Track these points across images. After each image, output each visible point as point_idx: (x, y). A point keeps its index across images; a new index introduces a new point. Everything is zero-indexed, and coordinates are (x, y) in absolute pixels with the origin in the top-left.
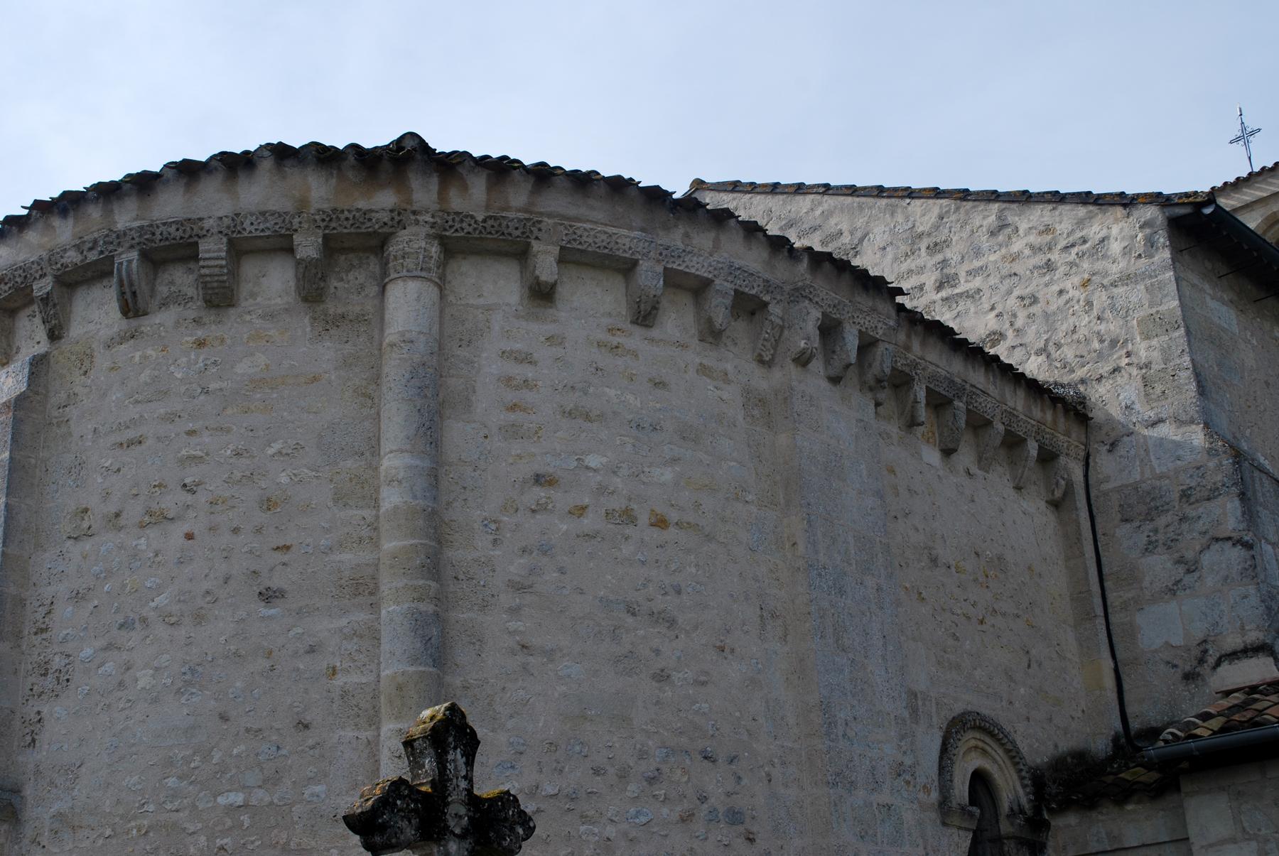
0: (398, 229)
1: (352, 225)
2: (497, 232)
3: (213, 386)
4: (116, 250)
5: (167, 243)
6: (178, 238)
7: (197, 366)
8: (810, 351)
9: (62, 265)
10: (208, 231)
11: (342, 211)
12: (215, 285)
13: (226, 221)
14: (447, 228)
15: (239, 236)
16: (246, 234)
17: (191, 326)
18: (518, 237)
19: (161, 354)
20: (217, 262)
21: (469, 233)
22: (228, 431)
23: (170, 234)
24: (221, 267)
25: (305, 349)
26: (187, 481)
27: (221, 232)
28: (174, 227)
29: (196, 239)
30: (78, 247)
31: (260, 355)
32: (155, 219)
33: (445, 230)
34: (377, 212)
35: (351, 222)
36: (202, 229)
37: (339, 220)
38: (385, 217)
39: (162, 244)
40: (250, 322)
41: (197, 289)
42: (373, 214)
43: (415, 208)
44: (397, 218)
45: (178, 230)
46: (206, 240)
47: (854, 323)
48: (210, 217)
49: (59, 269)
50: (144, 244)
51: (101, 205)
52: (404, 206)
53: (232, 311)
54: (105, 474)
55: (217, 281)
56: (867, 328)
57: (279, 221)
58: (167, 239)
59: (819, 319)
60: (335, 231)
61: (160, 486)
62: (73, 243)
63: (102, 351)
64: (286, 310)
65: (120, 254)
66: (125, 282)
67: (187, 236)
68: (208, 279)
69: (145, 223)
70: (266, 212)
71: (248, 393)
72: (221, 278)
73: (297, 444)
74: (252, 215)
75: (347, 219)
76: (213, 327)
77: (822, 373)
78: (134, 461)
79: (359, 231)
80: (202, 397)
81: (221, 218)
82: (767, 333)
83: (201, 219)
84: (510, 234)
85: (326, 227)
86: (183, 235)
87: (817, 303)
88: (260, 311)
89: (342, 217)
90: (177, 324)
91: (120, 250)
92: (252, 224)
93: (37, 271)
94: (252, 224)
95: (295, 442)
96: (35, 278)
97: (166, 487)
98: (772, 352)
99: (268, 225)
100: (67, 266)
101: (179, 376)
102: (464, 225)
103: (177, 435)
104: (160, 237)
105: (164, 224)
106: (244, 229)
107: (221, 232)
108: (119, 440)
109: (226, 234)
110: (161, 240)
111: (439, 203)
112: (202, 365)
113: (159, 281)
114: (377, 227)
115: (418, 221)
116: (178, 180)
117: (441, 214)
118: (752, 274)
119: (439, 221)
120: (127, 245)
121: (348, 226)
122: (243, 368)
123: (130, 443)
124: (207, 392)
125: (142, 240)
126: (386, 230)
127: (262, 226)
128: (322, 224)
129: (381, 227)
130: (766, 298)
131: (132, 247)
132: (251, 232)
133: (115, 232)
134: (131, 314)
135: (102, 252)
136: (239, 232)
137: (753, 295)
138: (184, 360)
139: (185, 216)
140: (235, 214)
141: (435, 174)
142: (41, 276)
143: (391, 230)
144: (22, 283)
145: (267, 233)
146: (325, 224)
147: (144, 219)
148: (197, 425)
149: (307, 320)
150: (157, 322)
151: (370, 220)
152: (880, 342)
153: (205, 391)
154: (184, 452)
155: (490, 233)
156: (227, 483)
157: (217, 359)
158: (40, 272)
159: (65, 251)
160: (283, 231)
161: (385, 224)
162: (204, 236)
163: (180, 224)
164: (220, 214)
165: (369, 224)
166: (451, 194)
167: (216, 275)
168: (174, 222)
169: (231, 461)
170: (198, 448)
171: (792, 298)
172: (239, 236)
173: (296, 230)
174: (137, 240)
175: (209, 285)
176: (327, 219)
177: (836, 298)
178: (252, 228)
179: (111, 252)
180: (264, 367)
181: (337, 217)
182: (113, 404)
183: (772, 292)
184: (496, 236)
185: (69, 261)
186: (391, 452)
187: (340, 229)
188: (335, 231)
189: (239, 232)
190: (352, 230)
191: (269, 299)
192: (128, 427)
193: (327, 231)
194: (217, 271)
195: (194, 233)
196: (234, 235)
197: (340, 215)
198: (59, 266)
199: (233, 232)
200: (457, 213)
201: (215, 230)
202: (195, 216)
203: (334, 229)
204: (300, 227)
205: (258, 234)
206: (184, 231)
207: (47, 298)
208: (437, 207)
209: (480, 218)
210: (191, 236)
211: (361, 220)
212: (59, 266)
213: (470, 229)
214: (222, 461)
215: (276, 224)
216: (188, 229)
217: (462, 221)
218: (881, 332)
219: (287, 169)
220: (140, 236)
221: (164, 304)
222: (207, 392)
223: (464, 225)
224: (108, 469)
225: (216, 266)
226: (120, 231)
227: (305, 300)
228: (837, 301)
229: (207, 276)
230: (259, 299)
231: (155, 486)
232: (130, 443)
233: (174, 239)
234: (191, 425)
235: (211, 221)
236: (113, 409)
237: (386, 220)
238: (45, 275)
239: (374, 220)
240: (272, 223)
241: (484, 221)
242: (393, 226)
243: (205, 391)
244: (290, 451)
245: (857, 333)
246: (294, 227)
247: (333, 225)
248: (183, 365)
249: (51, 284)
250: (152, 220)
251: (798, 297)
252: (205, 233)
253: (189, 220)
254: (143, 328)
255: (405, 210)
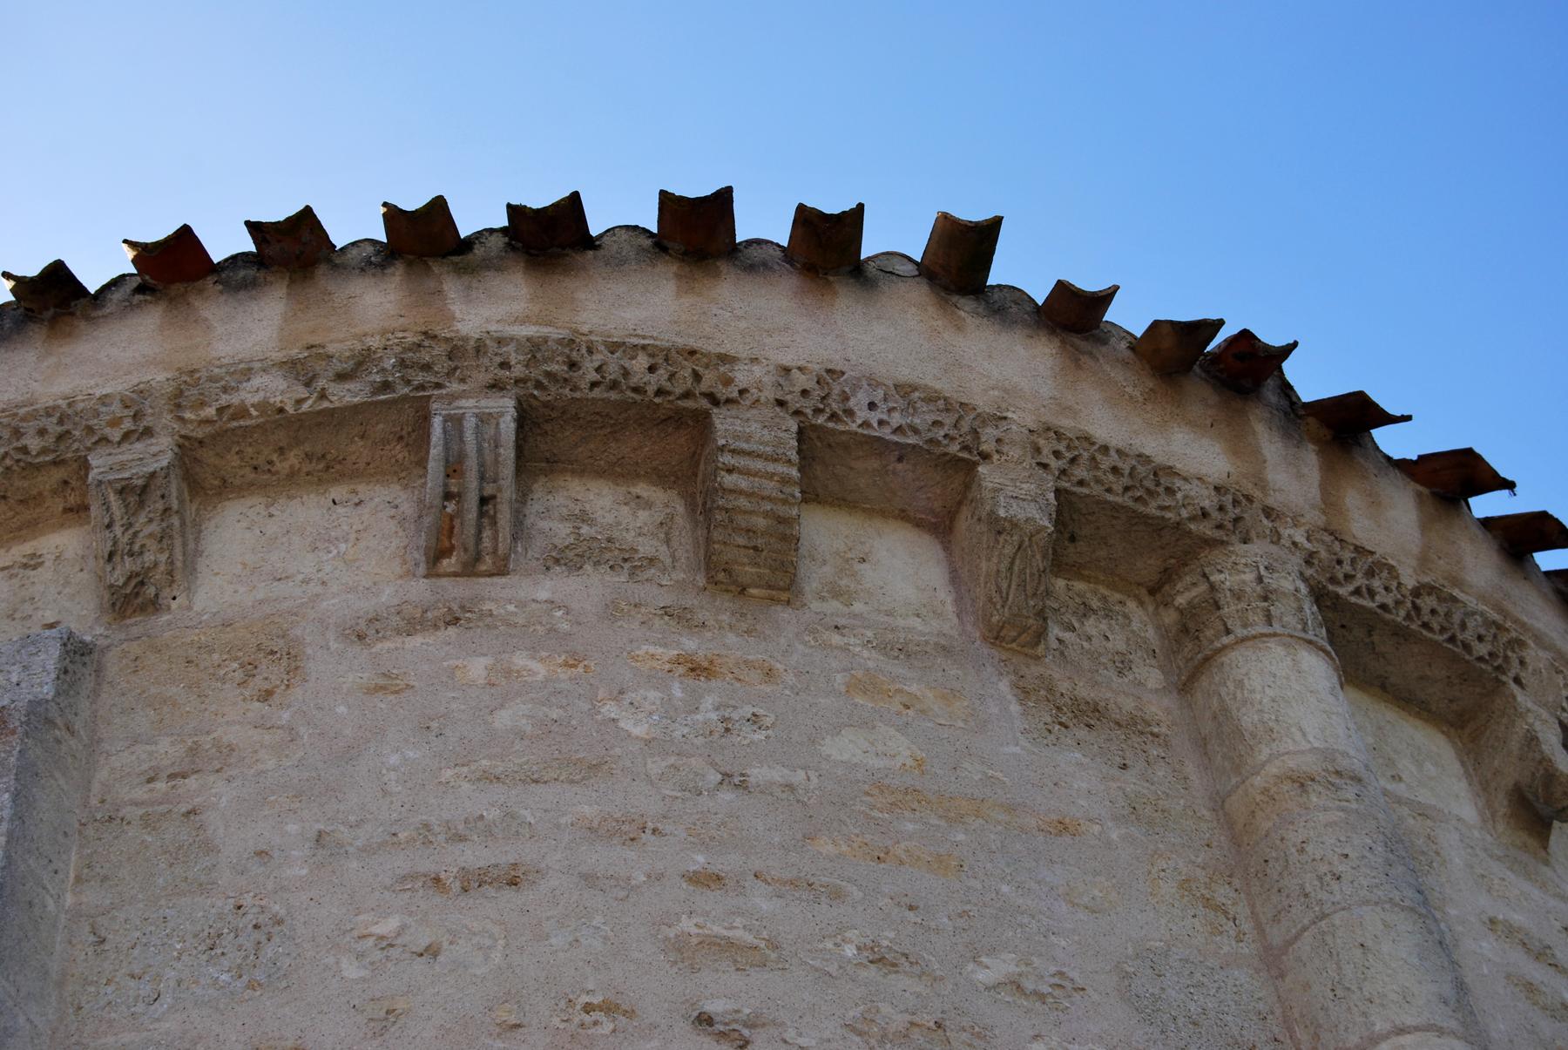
0: (1234, 539)
1: (1127, 489)
2: (1443, 630)
3: (757, 774)
4: (438, 386)
5: (614, 396)
6: (651, 390)
7: (699, 717)
9: (220, 410)
10: (742, 392)
11: (1105, 449)
12: (761, 523)
13: (802, 381)
14: (1340, 576)
15: (831, 425)
16: (854, 427)
17: (657, 622)
18: (1480, 659)
19: (564, 674)
20: (771, 467)
21: (1383, 607)
22: (836, 895)
23: (626, 373)
24: (785, 481)
25: (1017, 750)
26: (714, 1007)
27: (781, 403)
28: (642, 362)
29: (704, 403)
30: (292, 367)
31: (892, 731)
32: (585, 329)
33: (1333, 580)
34: (1185, 479)
35: (1126, 481)
36: (728, 382)
37: (1097, 468)
38: (1208, 500)
39: (596, 393)
40: (845, 649)
41: (668, 541)
42: (1178, 483)
43: (1270, 502)
44: (1233, 512)
45: (652, 369)
46: (734, 412)
48: (754, 360)
49: (208, 421)
50: (539, 385)
51: (398, 279)
52: (1249, 488)
53: (784, 614)
54: (378, 955)
55: (766, 515)
57: (948, 420)
58: (614, 385)
60: (1085, 491)
61: (609, 1008)
62: (278, 356)
63: (334, 645)
64: (944, 648)
65: (454, 397)
66: (472, 464)
67: (678, 391)
68: (743, 502)
69: (554, 333)
70: (915, 388)
71: (875, 813)
72: (782, 510)
73: (1061, 974)
74: (874, 383)
75: (1115, 470)
76: (731, 638)
78: (496, 930)
79: (1141, 509)
80: (727, 796)
81: (787, 370)
83: (724, 358)
84: (1467, 647)
85: (1063, 472)
86: (667, 386)
88: (869, 634)
89: (1106, 464)
90: (612, 611)
91: (455, 387)
92: (872, 406)
93: (114, 423)
94: (872, 406)
95: (1053, 969)
96: (104, 440)
97: (630, 1014)
99: (917, 421)
100: (242, 412)
101: (639, 731)
102: (1376, 584)
103: (656, 877)
104: (594, 376)
105: (613, 347)
106: (850, 413)
107: (781, 403)
108: (427, 866)
109: (797, 413)
110: (594, 385)
111: (1324, 513)
112: (714, 716)
113: (533, 508)
114: (1185, 513)
115: (1279, 537)
116: (654, 266)
117: (1328, 538)
119: (1323, 554)
120: (483, 378)
121: (1118, 488)
122: (844, 748)
123: (474, 881)
124: (742, 786)
125: (536, 373)
126: (1204, 529)
127: (896, 419)
128: (1054, 464)
129: (1192, 519)
131: (496, 386)
132: (866, 424)
133: (447, 340)
134: (449, 564)
135: (386, 386)
136: (834, 417)
138: (653, 695)
139: (680, 341)
140: (829, 371)
141: (1311, 447)
142: (126, 436)
143: (1218, 534)
144: (44, 451)
145: (912, 440)
146: (1061, 463)
147: (549, 324)
148: (727, 863)
149: (1004, 686)
150: (543, 595)
151: (1170, 491)
153: (735, 781)
154: (687, 925)
155: (1425, 625)
156: (860, 1034)
157: (760, 712)
158: (128, 425)
159: (248, 373)
160: (954, 448)
161: (1205, 514)
162: (729, 401)
163: (661, 357)
164: (787, 359)
165: (1168, 502)
166: (1347, 500)
167: (769, 499)
168: (644, 347)
169: (863, 974)
170: (738, 921)
172: (831, 425)
173: (985, 457)
174: (518, 371)
175: (741, 520)
176: (1069, 455)
178: (874, 417)
179: (422, 387)
180: (909, 762)
181: (1093, 459)
182: (393, 775)
184: (1440, 638)
185: (257, 399)
186: (1401, 1031)
187: (1097, 490)
188: (1085, 491)
189: (834, 417)
190: (1125, 500)
191: (889, 614)
192: (462, 839)
193: (1065, 484)
194: (770, 487)
195: (704, 386)
196: (820, 420)
197: (1099, 457)
198: (210, 412)
199: (817, 411)
200: (1359, 550)
201: (769, 394)
202: (712, 348)
203: (1081, 483)
204: (997, 451)
205: (886, 433)
206: (672, 376)
207: (145, 489)
208: (1321, 520)
209: (1409, 582)
210: (687, 395)
211: (1149, 484)
212: (210, 412)
213: (1389, 600)
214: (833, 969)
215: (935, 423)
216: (687, 373)
217: (1370, 573)
219: (962, 313)
220: (533, 360)
221: (562, 559)
222: (742, 786)
223: (1376, 584)
224: (385, 943)
225: (771, 476)
226: (465, 339)
227: (996, 637)
229: (741, 492)
230: (858, 607)
231: (588, 1008)
232: (474, 881)
233: (636, 390)
234: (701, 859)
235: (757, 370)
236: (395, 788)
237: (1206, 504)
238: (148, 432)
239: (1179, 495)
240: (930, 418)
241: (1416, 592)
242: (1219, 527)
243: (735, 781)
244: (1045, 989)
246: (984, 447)
247: (1080, 472)
248: (647, 706)
249: (170, 455)
250: (576, 331)
252: (735, 394)
253: (692, 353)
254: (487, 606)
255: (1249, 499)
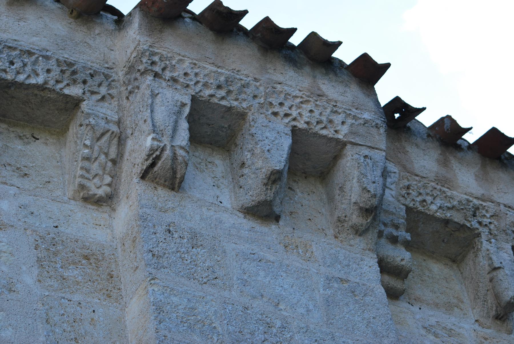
8: (168, 153)
47: (275, 114)
56: (308, 123)
59: (183, 105)
77: (227, 203)
82: (85, 146)
87: (174, 80)
98: (108, 179)
118: (30, 53)
130: (75, 91)
137: (36, 86)
152: (349, 147)
171: (130, 88)
177: (221, 74)
183: (85, 82)
218: (344, 130)
228: (222, 79)
245: (288, 130)
251: (136, 79)
